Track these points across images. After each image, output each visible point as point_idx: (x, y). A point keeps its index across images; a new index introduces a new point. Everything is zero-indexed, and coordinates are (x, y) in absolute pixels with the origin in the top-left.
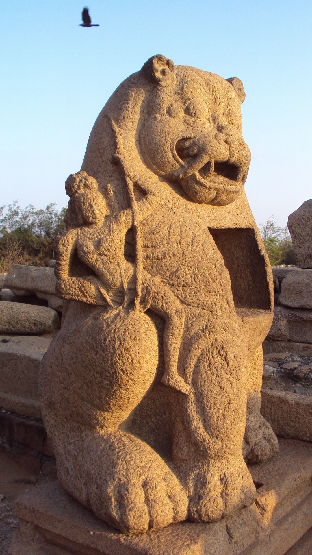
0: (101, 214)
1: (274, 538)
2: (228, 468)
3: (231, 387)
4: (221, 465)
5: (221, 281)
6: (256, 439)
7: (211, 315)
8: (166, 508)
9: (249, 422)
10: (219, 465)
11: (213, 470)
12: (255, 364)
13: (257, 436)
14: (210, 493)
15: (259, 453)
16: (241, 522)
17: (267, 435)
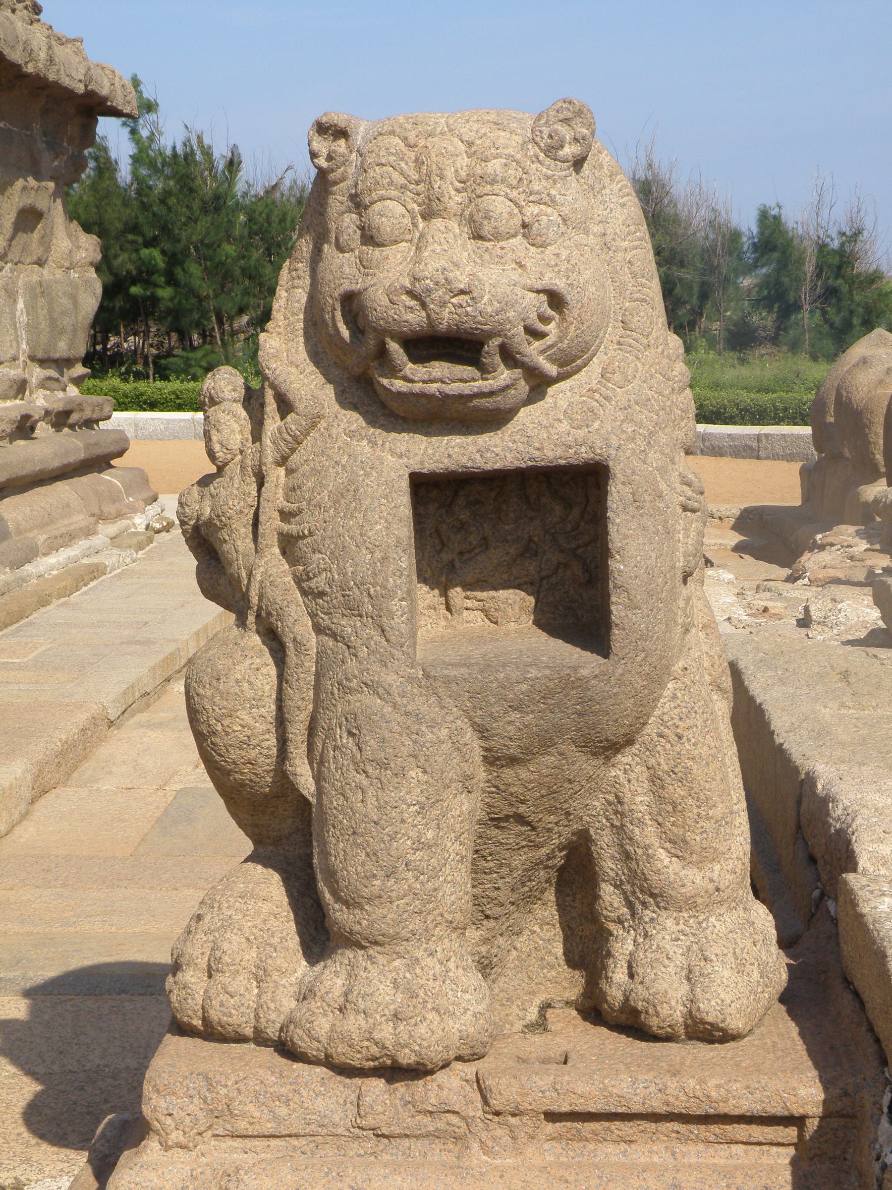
0: (225, 450)
1: (502, 1176)
2: (365, 969)
3: (362, 801)
4: (355, 957)
5: (372, 590)
6: (649, 970)
7: (347, 654)
8: (232, 1001)
9: (657, 927)
10: (351, 956)
11: (341, 964)
12: (663, 787)
13: (654, 965)
14: (313, 1002)
15: (640, 1005)
16: (410, 1099)
17: (697, 974)
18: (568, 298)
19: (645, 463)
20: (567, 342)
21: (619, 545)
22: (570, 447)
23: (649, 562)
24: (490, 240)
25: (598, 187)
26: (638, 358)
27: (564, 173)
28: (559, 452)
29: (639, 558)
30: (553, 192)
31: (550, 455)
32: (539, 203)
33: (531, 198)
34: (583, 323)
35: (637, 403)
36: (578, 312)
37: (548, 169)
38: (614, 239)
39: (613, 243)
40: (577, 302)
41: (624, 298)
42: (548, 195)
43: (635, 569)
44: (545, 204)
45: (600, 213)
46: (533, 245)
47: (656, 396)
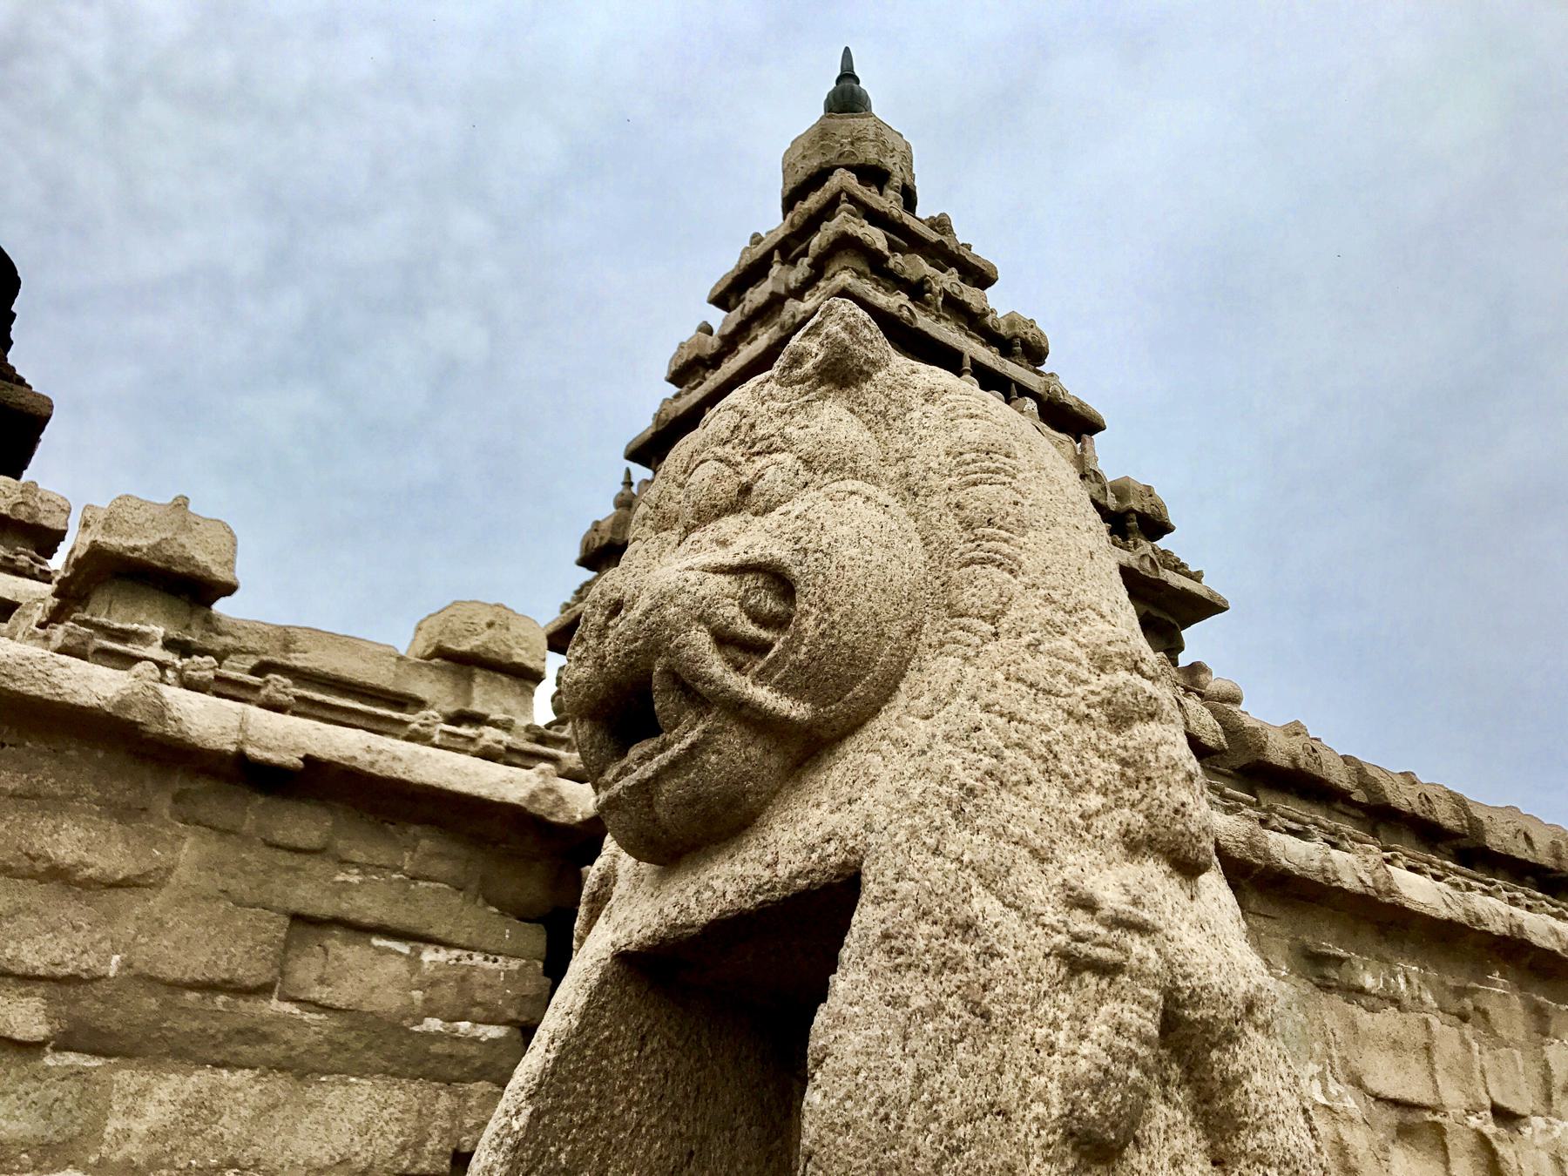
18: (796, 571)
19: (936, 852)
20: (804, 649)
21: (821, 1042)
22: (812, 849)
23: (890, 1088)
24: (694, 526)
25: (894, 411)
26: (966, 659)
27: (806, 398)
28: (798, 863)
29: (863, 1074)
30: (788, 430)
31: (783, 871)
32: (769, 451)
33: (755, 449)
34: (828, 610)
35: (947, 738)
36: (819, 592)
37: (783, 401)
38: (925, 479)
39: (921, 483)
40: (816, 576)
41: (948, 565)
42: (782, 435)
43: (849, 1104)
44: (776, 450)
45: (899, 446)
46: (756, 514)
47: (1000, 722)
